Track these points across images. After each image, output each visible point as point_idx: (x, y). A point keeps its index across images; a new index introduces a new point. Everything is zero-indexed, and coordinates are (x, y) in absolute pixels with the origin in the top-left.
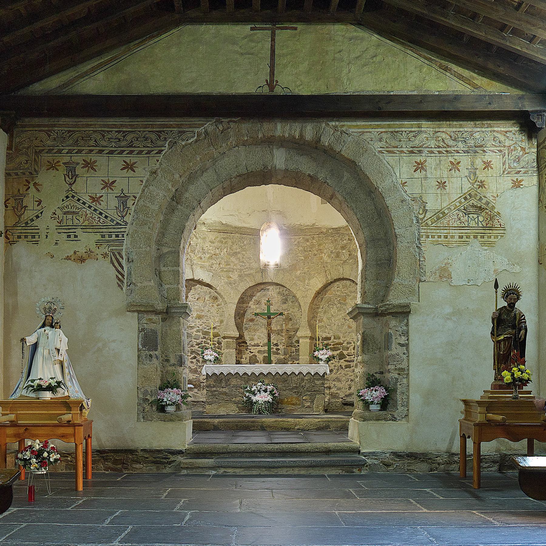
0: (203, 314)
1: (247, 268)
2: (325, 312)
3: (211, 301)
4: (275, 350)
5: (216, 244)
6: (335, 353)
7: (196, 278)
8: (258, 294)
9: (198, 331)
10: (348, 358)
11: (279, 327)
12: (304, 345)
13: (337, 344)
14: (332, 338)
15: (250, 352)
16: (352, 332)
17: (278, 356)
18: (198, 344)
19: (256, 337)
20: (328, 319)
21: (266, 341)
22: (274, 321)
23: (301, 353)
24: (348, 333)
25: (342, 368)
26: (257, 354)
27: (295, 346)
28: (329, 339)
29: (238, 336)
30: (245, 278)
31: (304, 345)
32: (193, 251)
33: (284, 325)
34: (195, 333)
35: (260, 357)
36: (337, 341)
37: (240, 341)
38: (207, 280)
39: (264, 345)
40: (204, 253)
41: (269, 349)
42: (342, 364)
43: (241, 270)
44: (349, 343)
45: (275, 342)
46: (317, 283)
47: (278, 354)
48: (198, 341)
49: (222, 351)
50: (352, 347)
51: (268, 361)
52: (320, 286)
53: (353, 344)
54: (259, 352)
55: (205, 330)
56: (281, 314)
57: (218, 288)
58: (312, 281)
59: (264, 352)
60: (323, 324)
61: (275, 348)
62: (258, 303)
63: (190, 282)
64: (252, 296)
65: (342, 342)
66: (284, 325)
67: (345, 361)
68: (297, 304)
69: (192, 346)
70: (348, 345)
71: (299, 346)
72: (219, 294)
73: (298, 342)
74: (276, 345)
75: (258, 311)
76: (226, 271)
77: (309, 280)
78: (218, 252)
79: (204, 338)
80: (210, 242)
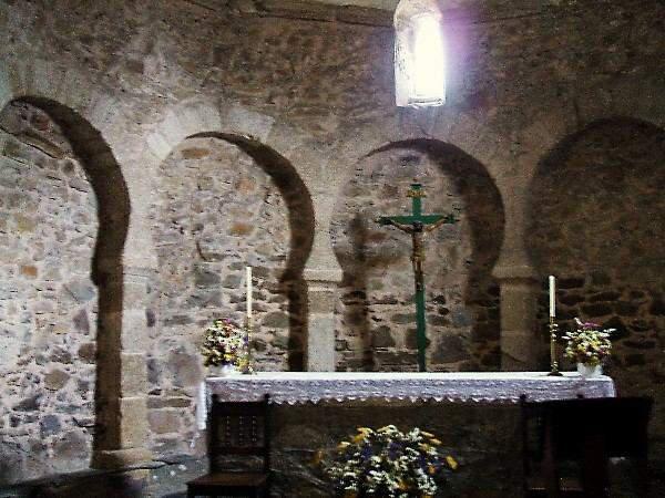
1: (361, 106)
2: (566, 213)
4: (436, 313)
9: (237, 266)
10: (635, 337)
15: (374, 319)
19: (386, 280)
20: (577, 229)
23: (504, 323)
26: (390, 324)
27: (488, 303)
28: (579, 283)
30: (357, 130)
36: (600, 289)
39: (409, 301)
41: (421, 308)
44: (635, 294)
45: (437, 293)
47: (444, 322)
49: (300, 318)
50: (646, 307)
52: (550, 141)
54: (398, 318)
59: (409, 318)
60: (560, 243)
65: (615, 291)
67: (628, 344)
71: (498, 302)
73: (495, 291)
74: (441, 300)
75: (391, 213)
76: (307, 113)
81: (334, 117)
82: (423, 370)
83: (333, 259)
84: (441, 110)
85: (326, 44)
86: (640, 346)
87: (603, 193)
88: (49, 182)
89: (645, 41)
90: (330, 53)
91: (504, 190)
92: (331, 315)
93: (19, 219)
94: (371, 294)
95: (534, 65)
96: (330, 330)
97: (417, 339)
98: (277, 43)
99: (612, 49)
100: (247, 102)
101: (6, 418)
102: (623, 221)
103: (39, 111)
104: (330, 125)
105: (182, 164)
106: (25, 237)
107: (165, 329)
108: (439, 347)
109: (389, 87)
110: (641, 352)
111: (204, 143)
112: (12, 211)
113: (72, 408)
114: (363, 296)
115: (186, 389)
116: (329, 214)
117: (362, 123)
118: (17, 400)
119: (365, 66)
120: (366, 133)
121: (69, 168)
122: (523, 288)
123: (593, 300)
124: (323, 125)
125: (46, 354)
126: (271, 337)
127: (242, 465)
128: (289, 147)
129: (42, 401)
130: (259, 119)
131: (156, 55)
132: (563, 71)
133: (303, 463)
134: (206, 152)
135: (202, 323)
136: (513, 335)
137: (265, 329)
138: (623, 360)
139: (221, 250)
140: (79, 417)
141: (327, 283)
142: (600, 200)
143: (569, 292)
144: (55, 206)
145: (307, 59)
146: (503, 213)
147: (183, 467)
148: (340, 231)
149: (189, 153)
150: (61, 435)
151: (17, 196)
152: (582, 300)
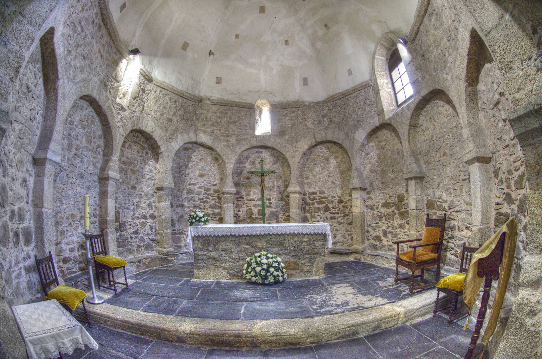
0: (205, 172)
2: (311, 170)
3: (213, 161)
4: (268, 204)
5: (218, 114)
6: (321, 206)
7: (199, 141)
8: (253, 156)
9: (200, 188)
11: (271, 184)
12: (295, 199)
13: (323, 198)
14: (318, 193)
16: (336, 187)
17: (270, 209)
18: (200, 199)
20: (314, 176)
21: (260, 196)
22: (266, 179)
23: (291, 207)
24: (331, 189)
25: (327, 219)
26: (253, 208)
27: (285, 201)
28: (315, 193)
29: (235, 192)
31: (295, 199)
32: (198, 119)
33: (275, 182)
34: (197, 190)
35: (255, 210)
36: (322, 195)
37: (238, 196)
38: (210, 144)
39: (259, 200)
40: (207, 121)
42: (328, 216)
43: (238, 135)
44: (332, 197)
45: (268, 197)
46: (304, 145)
47: (270, 207)
48: (200, 197)
49: (222, 206)
50: (336, 201)
51: (262, 217)
52: (306, 147)
53: (337, 198)
54: (254, 206)
55: (207, 187)
56: (273, 172)
57: (218, 150)
58: (299, 144)
59: (259, 206)
60: (309, 180)
61: (268, 202)
62: (253, 163)
63: (195, 145)
64: (247, 158)
66: (275, 182)
67: (331, 213)
68: (286, 164)
69: (194, 201)
70: (333, 199)
72: (219, 155)
73: (288, 196)
74: (269, 199)
75: (253, 170)
76: (226, 136)
77: (297, 142)
78: (219, 120)
79: (206, 194)
80: (213, 112)
81: (234, 137)
82: (264, 223)
83: (233, 185)
84: (270, 136)
85: (232, 114)
86: (334, 214)
87: (322, 164)
88: (140, 158)
89: (335, 117)
90: (233, 117)
91: (291, 163)
92: (232, 205)
93: (131, 170)
94: (245, 198)
95: (300, 123)
96: (232, 209)
97: (262, 213)
98: (216, 113)
99: (325, 119)
100: (205, 132)
101: (129, 236)
102: (330, 173)
103: (139, 135)
104: (233, 140)
105: (183, 153)
106: (133, 176)
107: (177, 209)
108: (269, 216)
109: (253, 128)
110: (336, 215)
111: (190, 146)
112: (130, 167)
113: (148, 235)
114: (243, 198)
115: (184, 229)
116: (231, 170)
117: (243, 140)
118: (132, 231)
119: (245, 121)
120: (244, 143)
121: (147, 153)
122: (297, 195)
123: (319, 199)
124: (230, 140)
125: (139, 216)
126: (212, 212)
127: (205, 255)
128: (219, 147)
129: (139, 231)
130: (208, 137)
131: (177, 116)
132: (310, 125)
133: (226, 254)
134: (191, 149)
135: (189, 207)
136: (294, 211)
137: (210, 209)
138: (329, 219)
139: (195, 182)
140: (150, 237)
141: (231, 194)
142: (321, 167)
143: (312, 197)
144: (142, 166)
145: (225, 119)
146: (291, 171)
147: (184, 255)
148: (235, 176)
149: (185, 149)
150: (145, 243)
151: (131, 162)
152: (316, 199)
